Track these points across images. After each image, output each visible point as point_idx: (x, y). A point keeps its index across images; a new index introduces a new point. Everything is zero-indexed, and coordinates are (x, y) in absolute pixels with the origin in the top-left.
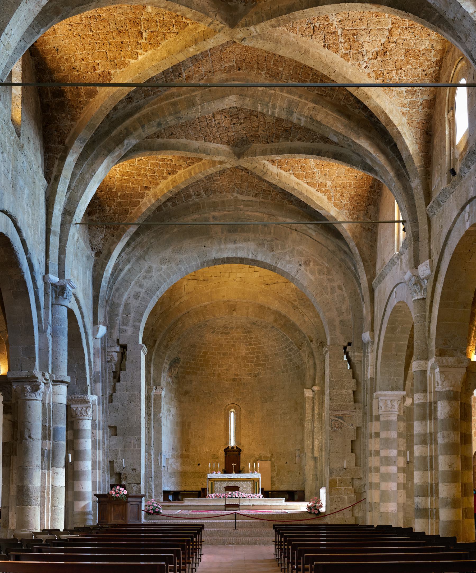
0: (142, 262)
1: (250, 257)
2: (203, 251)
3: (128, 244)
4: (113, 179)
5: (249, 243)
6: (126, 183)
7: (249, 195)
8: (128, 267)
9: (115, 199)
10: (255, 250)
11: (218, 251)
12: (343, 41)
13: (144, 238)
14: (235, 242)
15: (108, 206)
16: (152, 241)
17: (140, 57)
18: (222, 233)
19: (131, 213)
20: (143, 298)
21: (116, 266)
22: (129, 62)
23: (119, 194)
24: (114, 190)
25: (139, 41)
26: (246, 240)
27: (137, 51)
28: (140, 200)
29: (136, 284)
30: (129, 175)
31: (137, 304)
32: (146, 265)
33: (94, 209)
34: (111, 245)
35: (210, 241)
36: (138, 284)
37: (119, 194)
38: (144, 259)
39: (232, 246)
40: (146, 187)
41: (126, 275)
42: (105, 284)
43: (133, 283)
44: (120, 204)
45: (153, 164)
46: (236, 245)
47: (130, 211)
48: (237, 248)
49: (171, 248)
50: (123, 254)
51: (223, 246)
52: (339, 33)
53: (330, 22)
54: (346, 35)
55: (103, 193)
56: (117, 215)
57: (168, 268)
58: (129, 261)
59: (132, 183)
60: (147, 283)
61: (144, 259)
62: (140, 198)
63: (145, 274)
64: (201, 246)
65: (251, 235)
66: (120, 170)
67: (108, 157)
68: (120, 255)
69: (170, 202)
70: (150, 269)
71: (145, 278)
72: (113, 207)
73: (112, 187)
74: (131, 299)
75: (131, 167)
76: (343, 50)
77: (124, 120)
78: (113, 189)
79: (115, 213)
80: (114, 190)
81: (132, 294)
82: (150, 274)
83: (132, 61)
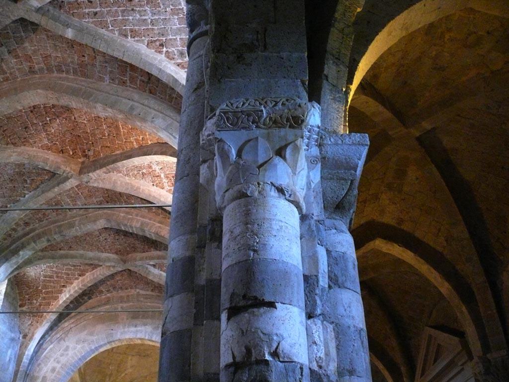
0: (62, 342)
1: (147, 338)
2: (111, 334)
3: (51, 329)
4: (38, 280)
5: (147, 327)
6: (48, 283)
7: (148, 290)
8: (51, 346)
9: (41, 295)
10: (151, 332)
11: (122, 333)
12: (166, 181)
13: (66, 324)
14: (136, 326)
15: (35, 300)
16: (72, 326)
17: (27, 196)
18: (127, 319)
19: (52, 305)
20: (58, 372)
21: (40, 345)
22: (20, 199)
23: (44, 291)
24: (40, 288)
25: (25, 186)
26: (145, 325)
27: (25, 192)
28: (60, 295)
29: (54, 360)
30: (50, 277)
31: (52, 377)
32: (64, 344)
33: (24, 302)
34: (35, 330)
35: (117, 325)
36: (57, 360)
37: (44, 291)
38: (64, 341)
39: (133, 329)
40: (63, 286)
41: (47, 353)
42: (26, 361)
43: (52, 360)
44: (44, 298)
45: (67, 269)
46: (135, 329)
47: (52, 303)
48: (137, 331)
49: (86, 331)
50: (46, 336)
51: (126, 330)
52: (162, 176)
53: (153, 169)
54: (167, 177)
55: (31, 290)
56: (42, 307)
57: (81, 348)
58: (52, 343)
59: (53, 282)
60: (63, 360)
61: (64, 341)
62: (59, 293)
63: (62, 352)
64: (110, 330)
65: (149, 321)
66: (43, 274)
67: (5, 264)
68: (42, 338)
69: (86, 296)
70: (67, 349)
71: (62, 355)
72: (39, 300)
73: (38, 286)
74: (48, 373)
75: (51, 272)
76: (167, 187)
77: (21, 238)
78: (39, 287)
79: (40, 305)
80: (40, 288)
81: (51, 368)
82: (67, 353)
83: (21, 199)
